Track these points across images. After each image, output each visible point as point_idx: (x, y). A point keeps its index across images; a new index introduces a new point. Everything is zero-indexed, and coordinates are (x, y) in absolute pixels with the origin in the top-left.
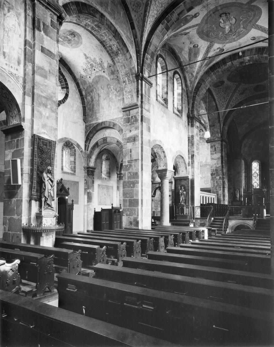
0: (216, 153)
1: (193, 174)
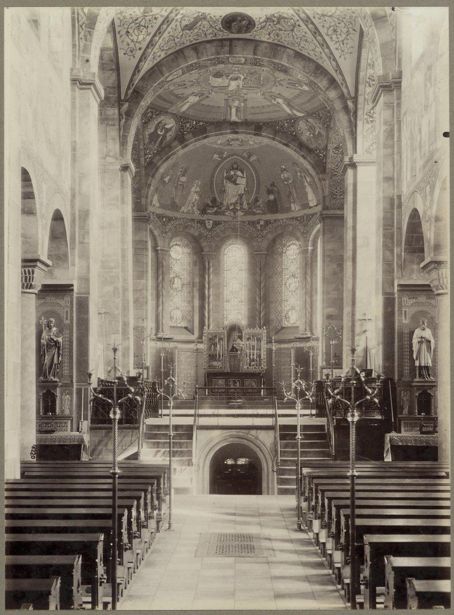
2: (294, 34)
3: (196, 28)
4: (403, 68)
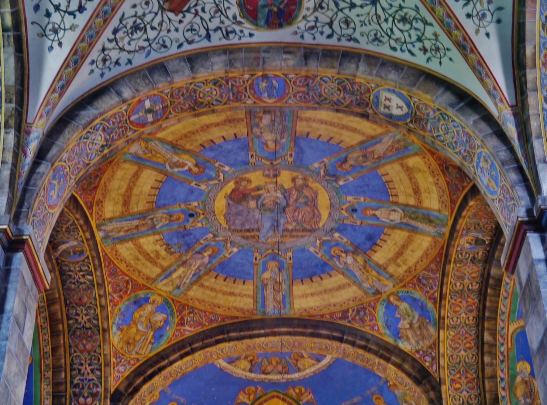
2: (380, 11)
3: (188, 11)
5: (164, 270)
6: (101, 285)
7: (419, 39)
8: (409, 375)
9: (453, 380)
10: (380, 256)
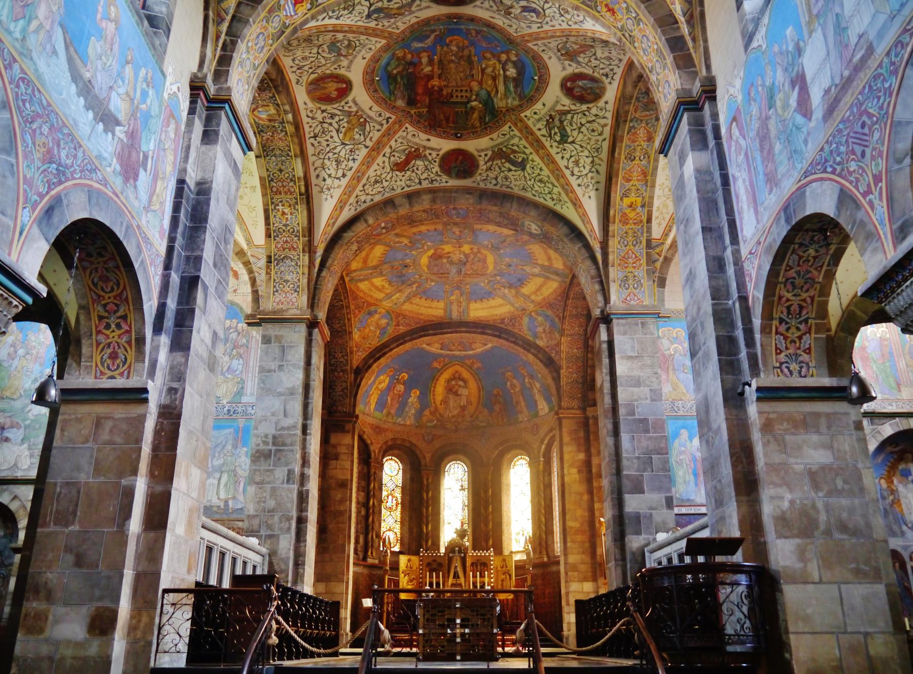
0: (281, 367)
1: (175, 385)
2: (526, 174)
4: (716, 70)
5: (387, 294)
6: (348, 307)
7: (550, 193)
8: (541, 361)
9: (568, 367)
10: (526, 290)
